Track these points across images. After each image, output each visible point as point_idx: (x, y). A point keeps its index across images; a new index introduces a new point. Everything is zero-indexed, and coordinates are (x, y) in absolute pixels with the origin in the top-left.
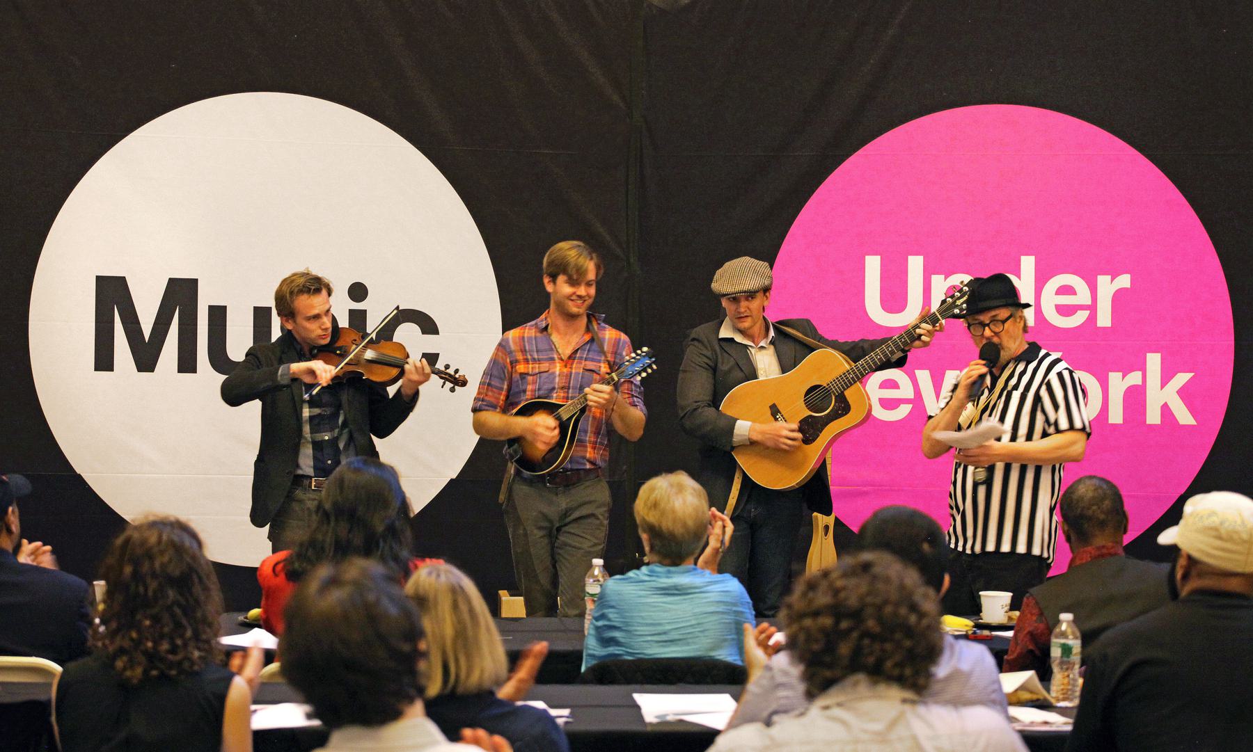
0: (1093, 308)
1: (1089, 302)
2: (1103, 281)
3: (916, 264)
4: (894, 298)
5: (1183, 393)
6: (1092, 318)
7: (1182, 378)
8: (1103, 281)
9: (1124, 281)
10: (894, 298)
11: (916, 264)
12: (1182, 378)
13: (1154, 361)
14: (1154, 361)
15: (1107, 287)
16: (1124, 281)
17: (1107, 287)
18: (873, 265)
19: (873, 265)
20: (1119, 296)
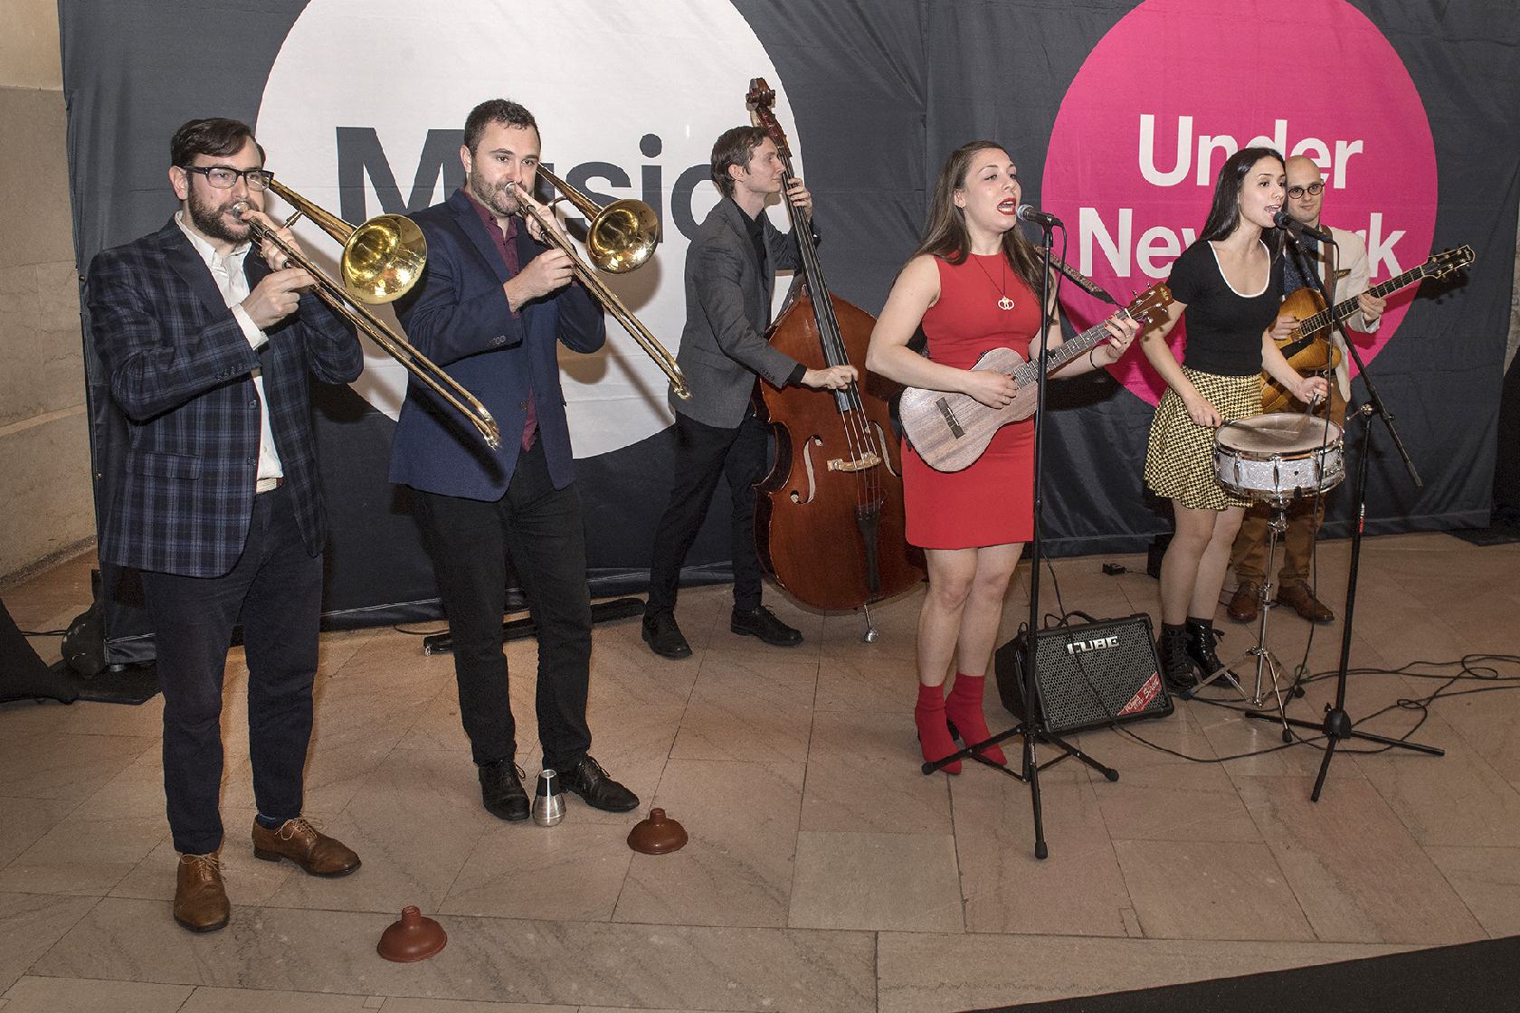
0: (1331, 171)
1: (1328, 165)
2: (1341, 145)
3: (1185, 124)
4: (1165, 160)
5: (1395, 249)
6: (1331, 179)
7: (1396, 236)
8: (1341, 145)
9: (1358, 146)
10: (1165, 160)
11: (1185, 124)
12: (1396, 236)
13: (1376, 219)
14: (1376, 219)
15: (1345, 150)
16: (1358, 146)
17: (1345, 150)
18: (1147, 123)
19: (1147, 123)
20: (1353, 160)
